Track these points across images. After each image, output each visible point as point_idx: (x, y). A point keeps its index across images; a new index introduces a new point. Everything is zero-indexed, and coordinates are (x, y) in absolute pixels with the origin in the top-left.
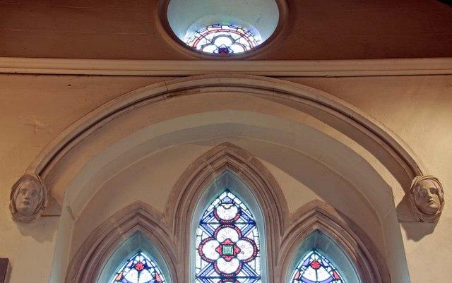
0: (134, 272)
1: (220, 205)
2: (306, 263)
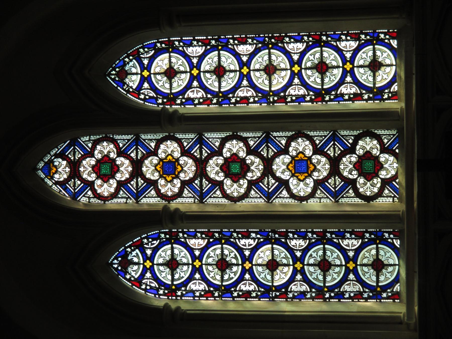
0: (129, 270)
1: (52, 178)
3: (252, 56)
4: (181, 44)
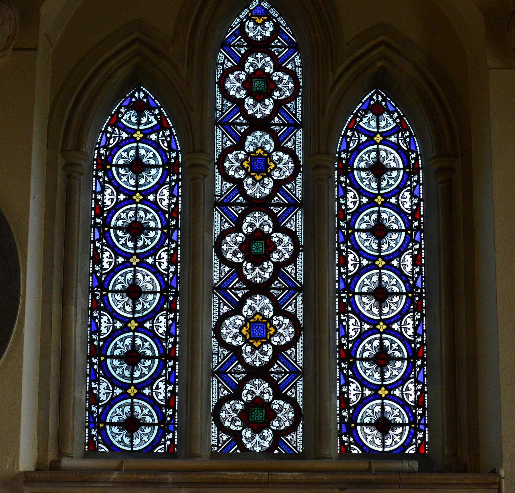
0: (132, 112)
1: (249, 18)
2: (365, 107)
3: (399, 272)
4: (415, 184)
